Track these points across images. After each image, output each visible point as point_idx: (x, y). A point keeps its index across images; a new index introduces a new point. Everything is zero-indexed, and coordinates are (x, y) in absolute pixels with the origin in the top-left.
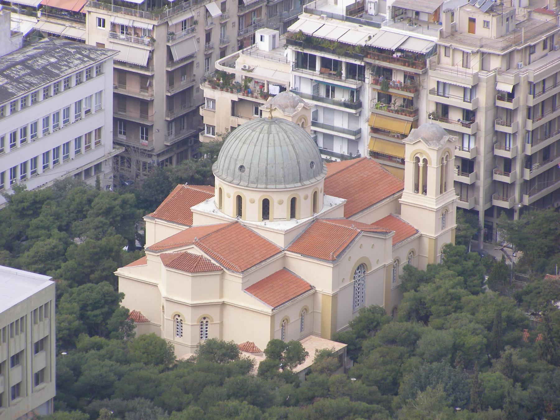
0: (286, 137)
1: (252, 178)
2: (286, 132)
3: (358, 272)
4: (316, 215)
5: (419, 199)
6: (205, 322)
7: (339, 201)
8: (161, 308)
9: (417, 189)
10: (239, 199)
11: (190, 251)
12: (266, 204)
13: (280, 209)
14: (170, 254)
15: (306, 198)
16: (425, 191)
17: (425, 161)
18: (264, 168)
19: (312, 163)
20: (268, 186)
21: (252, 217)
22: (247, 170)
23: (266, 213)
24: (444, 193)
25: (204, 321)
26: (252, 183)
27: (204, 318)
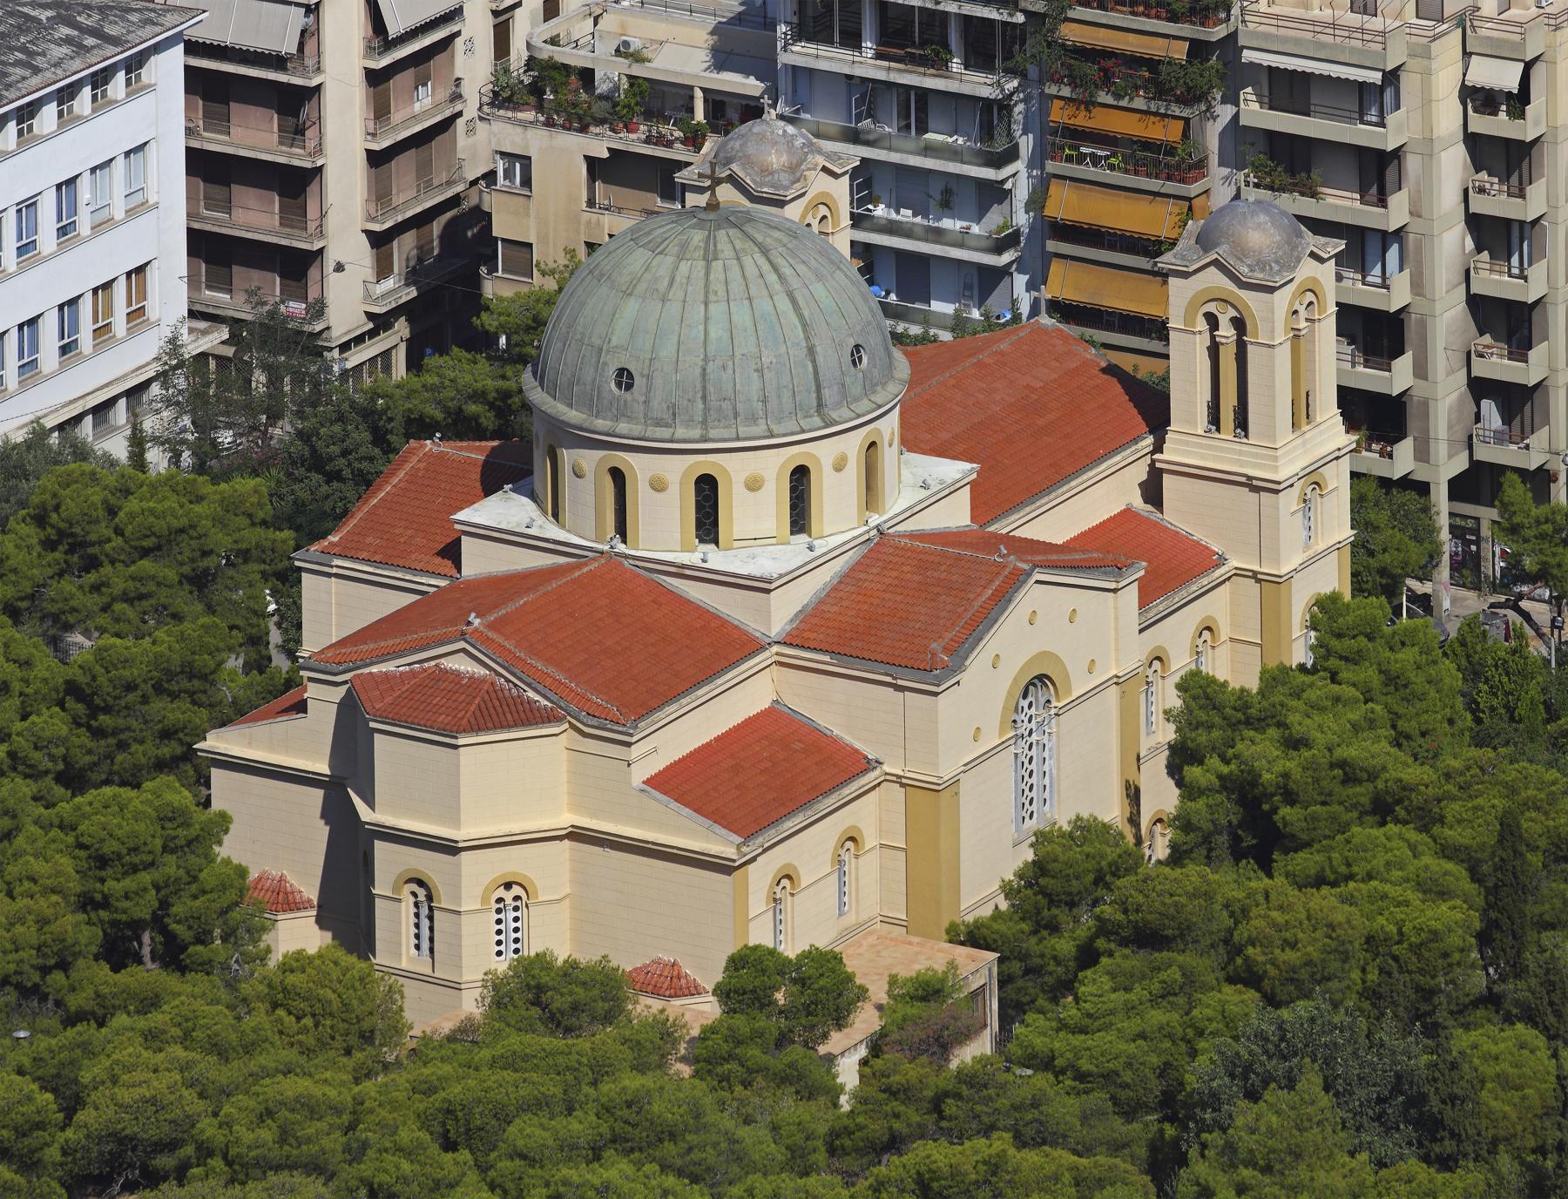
0: (766, 267)
1: (658, 407)
2: (765, 252)
3: (1025, 703)
4: (875, 520)
5: (1225, 453)
6: (509, 900)
7: (955, 470)
8: (361, 856)
9: (1215, 419)
10: (618, 475)
11: (452, 663)
12: (707, 490)
13: (753, 510)
14: (387, 676)
15: (839, 467)
16: (1242, 423)
17: (1239, 324)
18: (698, 371)
19: (857, 347)
20: (713, 433)
21: (662, 532)
22: (638, 381)
23: (707, 525)
24: (1305, 428)
25: (508, 896)
26: (659, 423)
27: (508, 886)
